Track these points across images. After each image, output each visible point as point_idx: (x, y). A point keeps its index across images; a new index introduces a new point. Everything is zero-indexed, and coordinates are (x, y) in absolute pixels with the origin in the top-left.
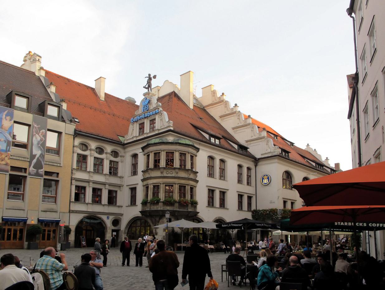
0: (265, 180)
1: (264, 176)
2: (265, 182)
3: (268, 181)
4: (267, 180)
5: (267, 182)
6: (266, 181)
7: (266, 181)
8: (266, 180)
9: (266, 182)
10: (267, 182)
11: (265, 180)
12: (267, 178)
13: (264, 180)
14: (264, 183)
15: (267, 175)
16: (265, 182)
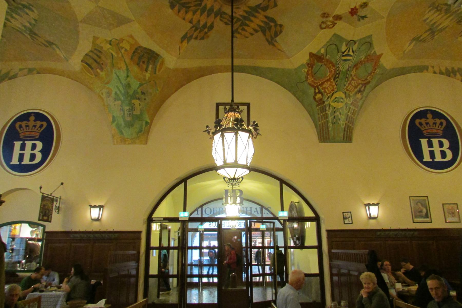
0: (23, 147)
1: (25, 117)
2: (21, 157)
3: (46, 152)
4: (40, 145)
5: (33, 157)
6: (28, 152)
7: (28, 152)
8: (29, 144)
9: (26, 161)
10: (33, 157)
11: (23, 147)
12: (37, 135)
13: (18, 144)
14: (15, 161)
15: (40, 117)
16: (21, 157)
